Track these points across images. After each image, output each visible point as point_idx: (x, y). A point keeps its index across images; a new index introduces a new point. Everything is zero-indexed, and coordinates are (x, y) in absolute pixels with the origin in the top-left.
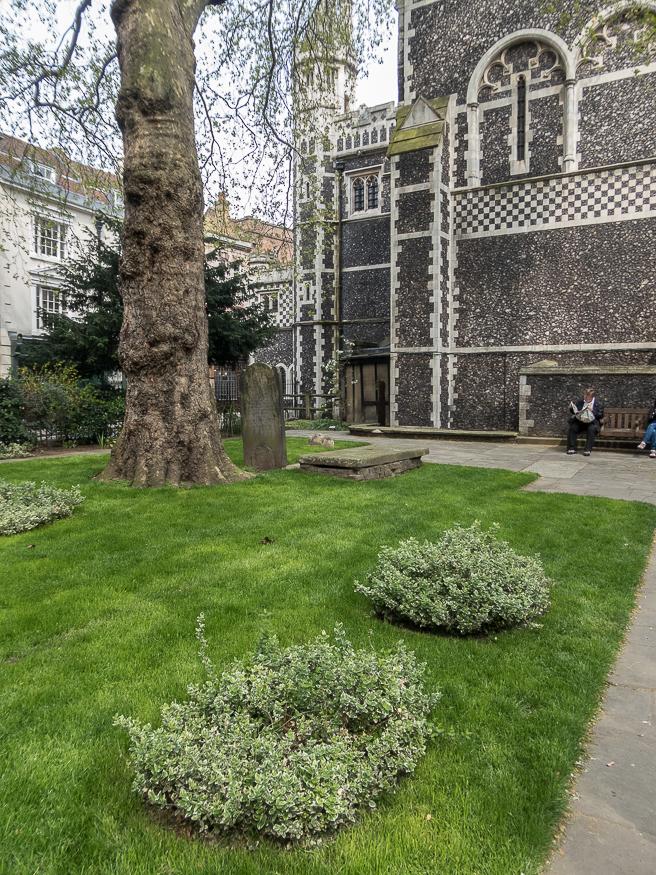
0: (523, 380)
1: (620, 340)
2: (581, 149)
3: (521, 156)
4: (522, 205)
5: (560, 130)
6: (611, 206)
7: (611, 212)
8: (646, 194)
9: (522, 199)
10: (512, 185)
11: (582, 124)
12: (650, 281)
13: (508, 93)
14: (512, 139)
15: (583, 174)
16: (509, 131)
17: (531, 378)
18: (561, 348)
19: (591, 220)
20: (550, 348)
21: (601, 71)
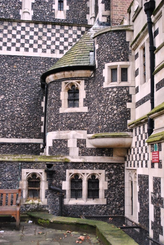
8: (5, 40)
12: (5, 96)
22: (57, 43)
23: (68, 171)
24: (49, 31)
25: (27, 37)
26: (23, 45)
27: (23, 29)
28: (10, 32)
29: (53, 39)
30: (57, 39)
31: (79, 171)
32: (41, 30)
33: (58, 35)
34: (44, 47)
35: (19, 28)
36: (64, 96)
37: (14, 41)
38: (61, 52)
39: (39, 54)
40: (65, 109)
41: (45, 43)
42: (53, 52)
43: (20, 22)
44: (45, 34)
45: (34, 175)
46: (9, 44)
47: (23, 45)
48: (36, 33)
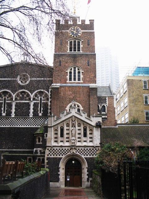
0: (2, 156)
1: (20, 149)
2: (15, 113)
3: (4, 112)
4: (4, 122)
5: (11, 109)
6: (19, 124)
7: (19, 125)
9: (4, 121)
10: (2, 118)
11: (15, 109)
13: (2, 100)
14: (3, 109)
15: (15, 118)
16: (2, 107)
17: (4, 156)
18: (10, 150)
19: (16, 126)
20: (8, 150)
21: (18, 100)
22: (39, 123)
23: (37, 158)
24: (37, 120)
25: (31, 122)
26: (30, 124)
27: (30, 120)
28: (27, 121)
29: (38, 122)
30: (39, 122)
31: (40, 157)
32: (35, 120)
33: (39, 121)
34: (36, 124)
35: (29, 120)
36: (37, 140)
37: (28, 123)
38: (40, 125)
39: (34, 126)
40: (37, 143)
41: (36, 123)
42: (38, 126)
43: (29, 118)
44: (36, 121)
45: (30, 158)
46: (26, 124)
47: (30, 124)
48: (33, 121)
